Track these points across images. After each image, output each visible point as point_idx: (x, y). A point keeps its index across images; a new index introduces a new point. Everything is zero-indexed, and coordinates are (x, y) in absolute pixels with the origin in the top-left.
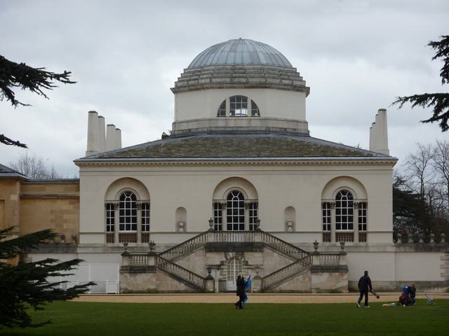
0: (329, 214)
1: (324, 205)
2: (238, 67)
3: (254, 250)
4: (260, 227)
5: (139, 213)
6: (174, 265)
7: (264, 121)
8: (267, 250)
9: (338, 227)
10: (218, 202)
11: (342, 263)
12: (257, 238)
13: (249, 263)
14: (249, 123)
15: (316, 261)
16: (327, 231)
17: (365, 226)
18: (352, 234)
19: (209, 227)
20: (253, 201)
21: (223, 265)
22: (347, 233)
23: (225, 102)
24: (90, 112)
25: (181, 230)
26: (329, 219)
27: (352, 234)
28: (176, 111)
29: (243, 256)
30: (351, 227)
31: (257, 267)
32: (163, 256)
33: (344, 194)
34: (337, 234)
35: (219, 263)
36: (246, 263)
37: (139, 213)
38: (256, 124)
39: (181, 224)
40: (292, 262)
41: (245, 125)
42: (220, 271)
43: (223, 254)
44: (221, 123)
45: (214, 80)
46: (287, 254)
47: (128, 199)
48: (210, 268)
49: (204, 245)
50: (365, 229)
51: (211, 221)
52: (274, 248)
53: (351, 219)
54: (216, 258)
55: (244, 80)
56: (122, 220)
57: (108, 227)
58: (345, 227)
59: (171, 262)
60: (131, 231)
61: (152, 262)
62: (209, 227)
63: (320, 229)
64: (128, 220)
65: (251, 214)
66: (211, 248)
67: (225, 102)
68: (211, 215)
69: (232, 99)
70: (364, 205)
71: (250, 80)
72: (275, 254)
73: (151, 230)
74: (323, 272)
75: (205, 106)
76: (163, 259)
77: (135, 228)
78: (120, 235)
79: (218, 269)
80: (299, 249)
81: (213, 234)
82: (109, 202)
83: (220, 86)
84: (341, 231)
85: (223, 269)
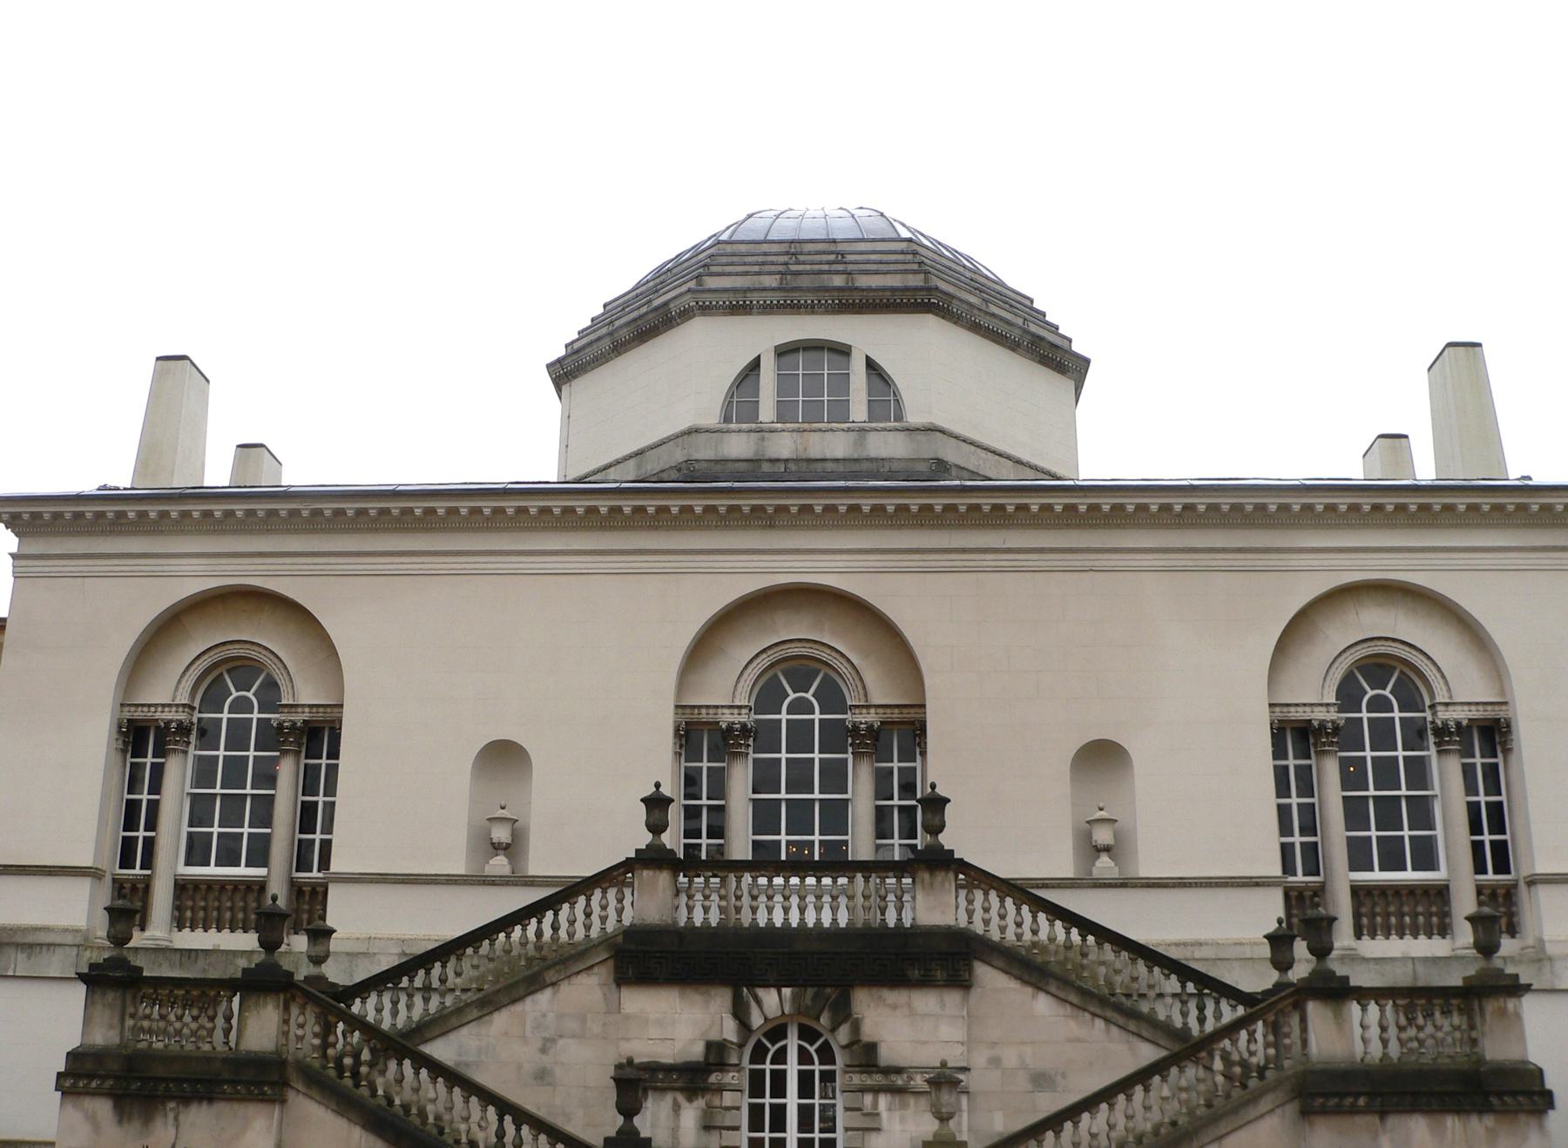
0: (1306, 788)
1: (1279, 732)
2: (810, 247)
3: (915, 974)
4: (946, 840)
5: (287, 771)
6: (422, 1061)
7: (920, 437)
8: (988, 976)
9: (1359, 857)
10: (704, 716)
11: (1496, 1049)
12: (933, 907)
13: (886, 1056)
14: (860, 443)
15: (1347, 1036)
16: (1300, 877)
17: (1500, 850)
18: (1440, 893)
19: (644, 839)
20: (896, 715)
21: (722, 1066)
22: (1412, 891)
23: (755, 365)
24: (158, 359)
25: (499, 865)
26: (1308, 812)
27: (1440, 893)
28: (565, 446)
29: (843, 1012)
30: (1425, 856)
31: (945, 1080)
32: (365, 1008)
33: (1382, 669)
34: (1358, 891)
35: (697, 1052)
36: (866, 1056)
37: (287, 771)
38: (887, 445)
39: (501, 834)
40: (1148, 1054)
41: (840, 454)
42: (700, 1103)
43: (721, 1000)
44: (738, 446)
45: (712, 283)
46: (1118, 1009)
47: (242, 705)
48: (634, 1083)
49: (607, 941)
50: (1502, 865)
51: (656, 804)
52: (1030, 968)
53: (1422, 813)
54: (677, 1022)
55: (838, 281)
56: (200, 811)
57: (128, 846)
58: (1392, 860)
59: (401, 1046)
60: (242, 871)
61: (262, 1028)
62: (645, 838)
63: (1275, 870)
64: (232, 814)
65: (883, 791)
66: (646, 958)
67: (755, 365)
68: (660, 767)
69: (784, 352)
70: (1493, 733)
71: (863, 281)
72: (1043, 1004)
73: (336, 865)
74: (1383, 1114)
75: (682, 388)
76: (357, 1023)
77: (260, 855)
78: (183, 888)
79: (692, 1092)
80: (1183, 972)
81: (664, 877)
82: (139, 714)
83: (739, 307)
84: (1377, 876)
85: (720, 1089)
